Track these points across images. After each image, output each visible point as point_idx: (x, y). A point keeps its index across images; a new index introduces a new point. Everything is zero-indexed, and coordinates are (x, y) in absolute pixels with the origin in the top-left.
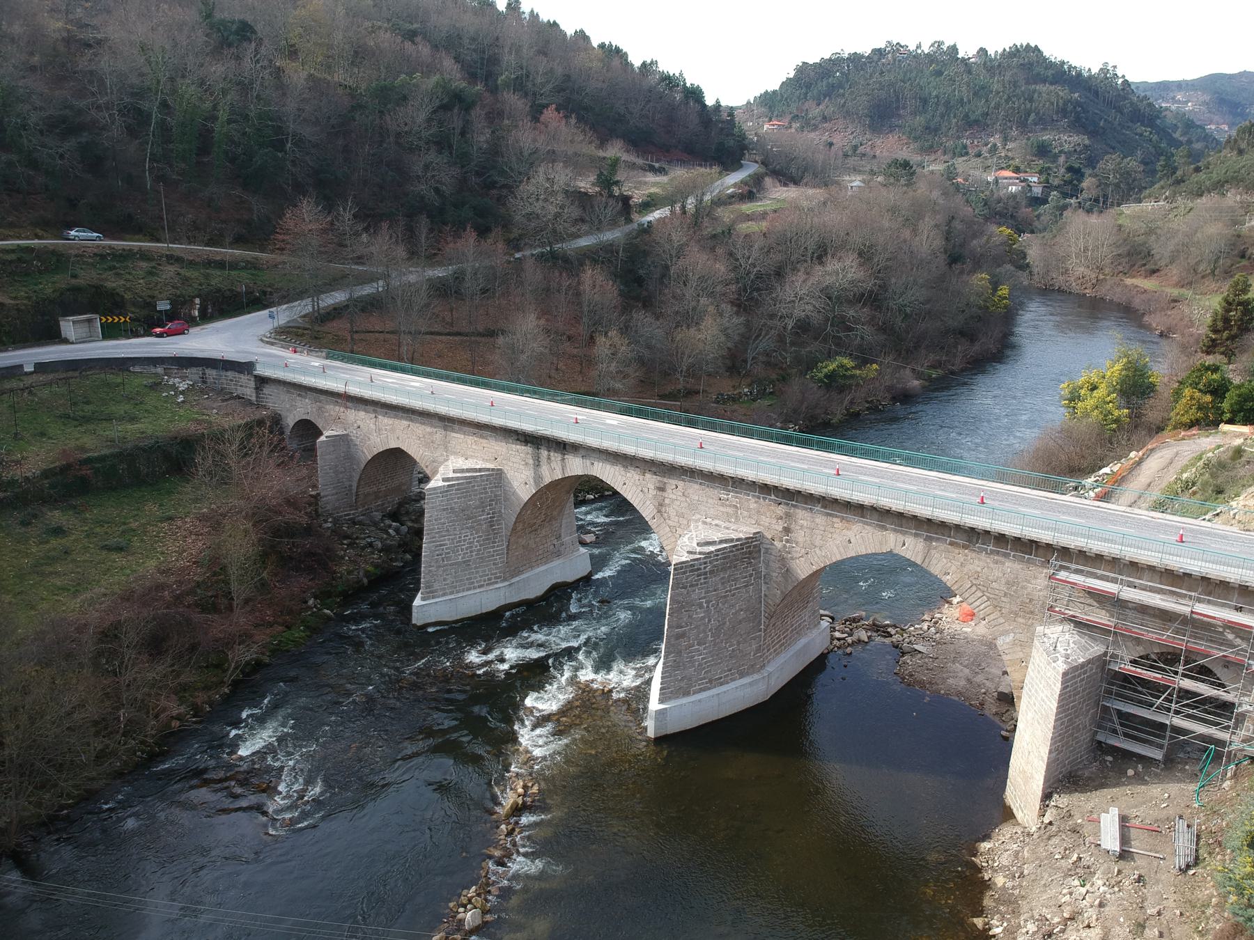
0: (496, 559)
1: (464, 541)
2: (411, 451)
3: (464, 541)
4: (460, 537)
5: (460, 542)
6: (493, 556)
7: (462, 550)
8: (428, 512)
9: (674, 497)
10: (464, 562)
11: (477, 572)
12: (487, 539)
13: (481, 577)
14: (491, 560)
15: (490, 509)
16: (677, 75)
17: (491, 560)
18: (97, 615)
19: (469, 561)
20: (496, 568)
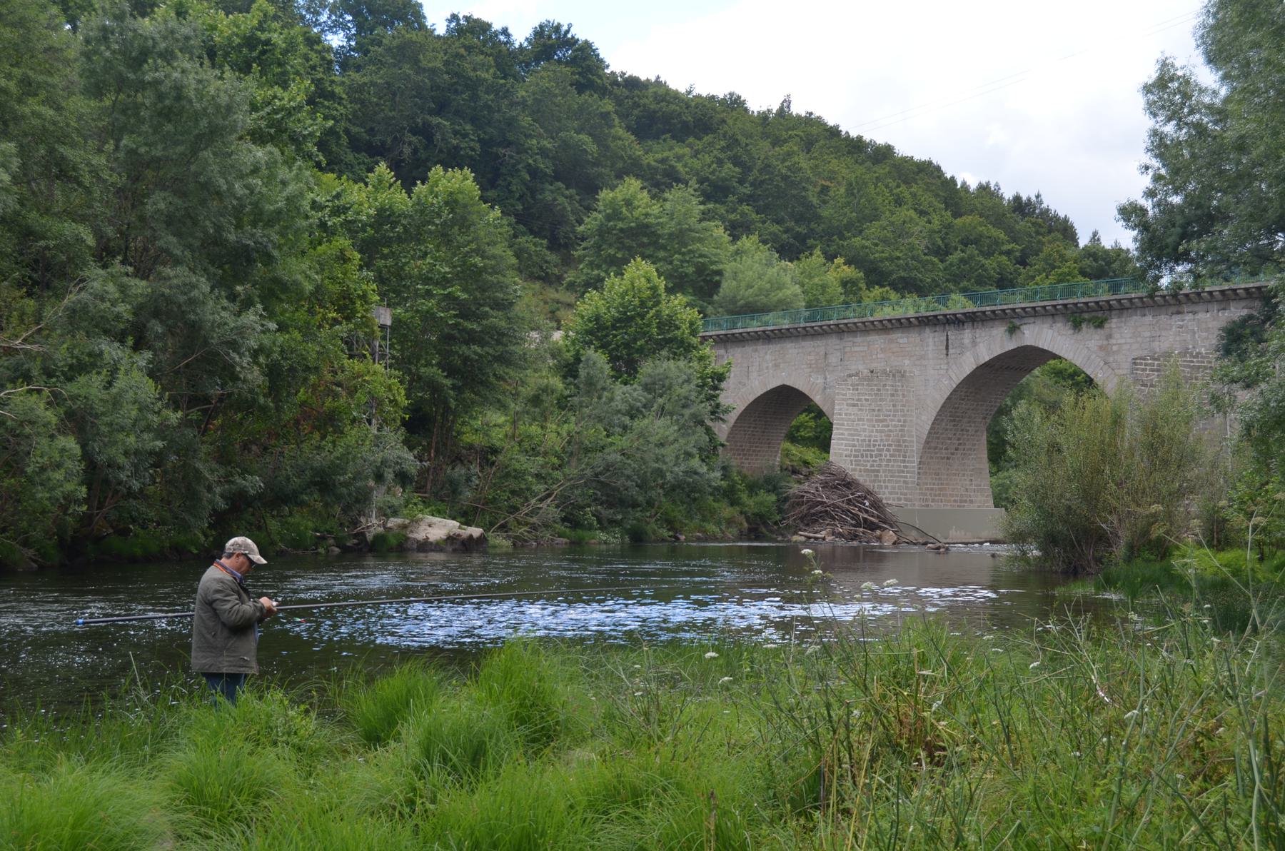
0: (906, 477)
1: (874, 446)
2: (800, 384)
3: (874, 446)
4: (870, 441)
5: (869, 445)
6: (903, 472)
7: (872, 456)
8: (839, 404)
9: (1123, 341)
10: (873, 471)
11: (886, 487)
12: (898, 451)
13: (891, 493)
14: (902, 477)
15: (903, 416)
16: (1033, 198)
17: (902, 477)
18: (729, 199)
19: (878, 471)
20: (907, 488)
